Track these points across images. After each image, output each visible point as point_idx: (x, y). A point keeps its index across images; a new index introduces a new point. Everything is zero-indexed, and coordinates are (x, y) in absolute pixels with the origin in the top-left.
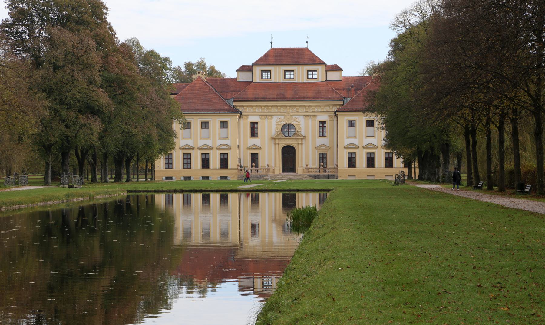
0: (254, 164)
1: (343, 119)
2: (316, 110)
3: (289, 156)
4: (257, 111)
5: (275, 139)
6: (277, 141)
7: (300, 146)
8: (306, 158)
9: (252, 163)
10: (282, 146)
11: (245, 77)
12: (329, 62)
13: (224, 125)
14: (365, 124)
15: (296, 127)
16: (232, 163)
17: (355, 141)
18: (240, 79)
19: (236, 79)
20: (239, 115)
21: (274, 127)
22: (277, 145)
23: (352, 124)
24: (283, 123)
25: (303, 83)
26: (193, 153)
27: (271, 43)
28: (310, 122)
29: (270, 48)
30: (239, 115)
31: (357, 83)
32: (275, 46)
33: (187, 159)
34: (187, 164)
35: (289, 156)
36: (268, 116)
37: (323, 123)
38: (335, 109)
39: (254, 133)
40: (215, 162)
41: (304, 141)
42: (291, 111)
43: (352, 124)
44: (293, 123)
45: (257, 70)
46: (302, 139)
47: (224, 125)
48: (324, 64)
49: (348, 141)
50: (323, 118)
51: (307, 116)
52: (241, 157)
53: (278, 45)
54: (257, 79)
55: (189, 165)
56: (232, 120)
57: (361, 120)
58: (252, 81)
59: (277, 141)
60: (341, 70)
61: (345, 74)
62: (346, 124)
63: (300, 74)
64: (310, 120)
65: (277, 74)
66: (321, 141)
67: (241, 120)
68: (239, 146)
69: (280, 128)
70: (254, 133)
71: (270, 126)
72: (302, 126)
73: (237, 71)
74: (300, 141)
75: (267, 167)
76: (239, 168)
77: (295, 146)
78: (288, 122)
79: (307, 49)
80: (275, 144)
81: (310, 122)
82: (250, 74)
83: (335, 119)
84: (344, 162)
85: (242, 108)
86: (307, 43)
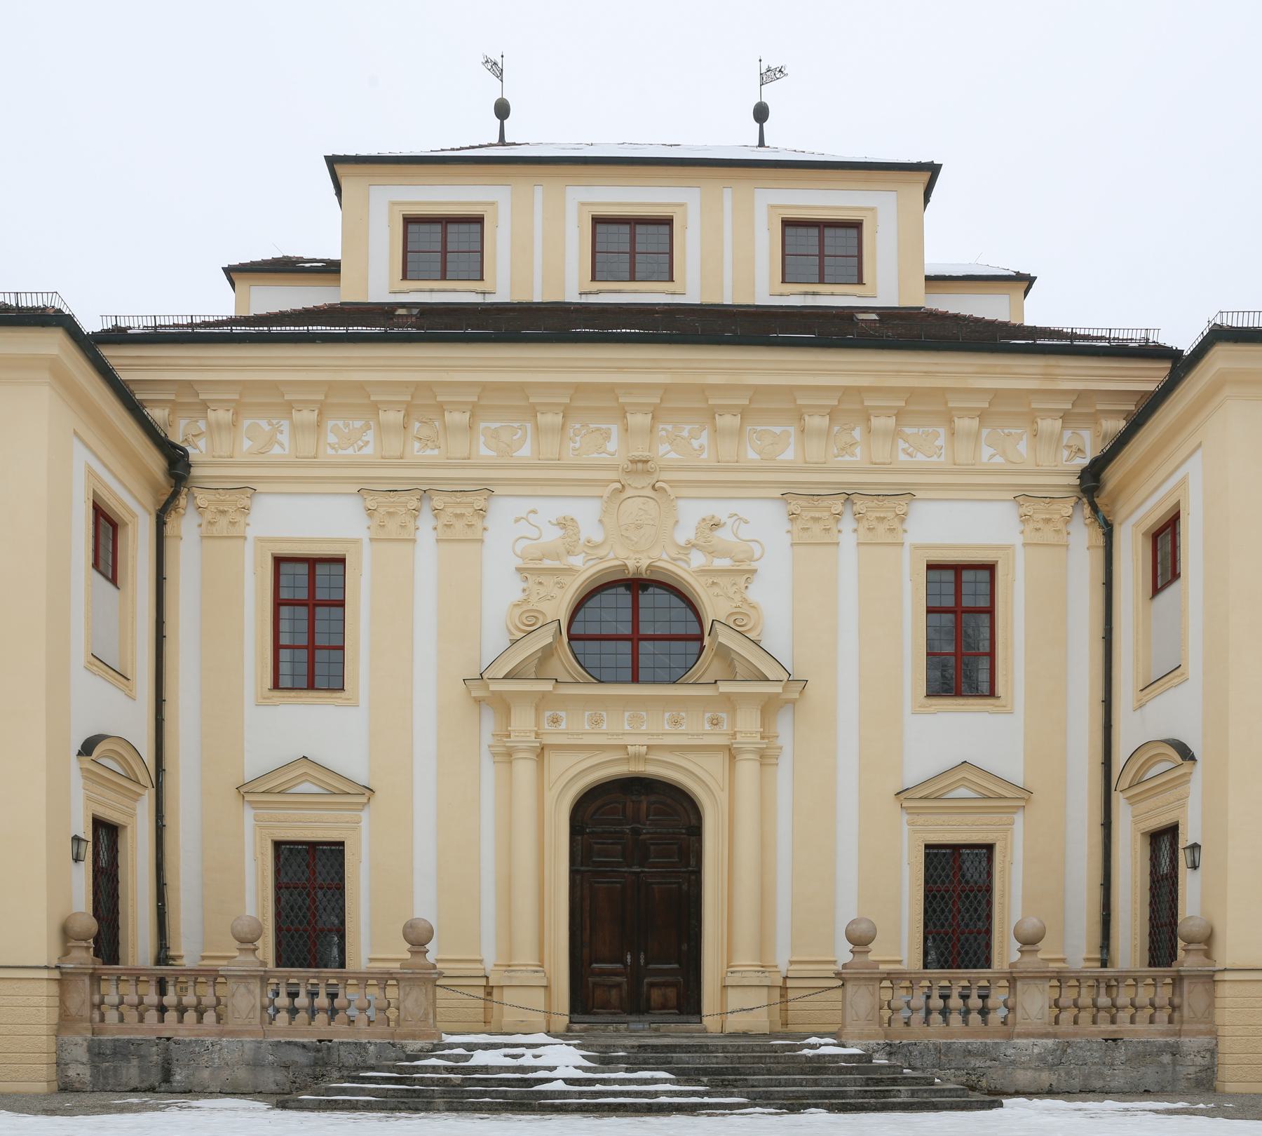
3: (636, 880)
5: (503, 705)
6: (523, 722)
7: (747, 769)
10: (573, 775)
15: (713, 606)
22: (524, 769)
24: (585, 569)
27: (502, 110)
35: (636, 880)
41: (784, 728)
44: (688, 569)
46: (769, 708)
51: (819, 503)
59: (523, 722)
71: (457, 594)
74: (748, 723)
78: (637, 561)
80: (507, 756)
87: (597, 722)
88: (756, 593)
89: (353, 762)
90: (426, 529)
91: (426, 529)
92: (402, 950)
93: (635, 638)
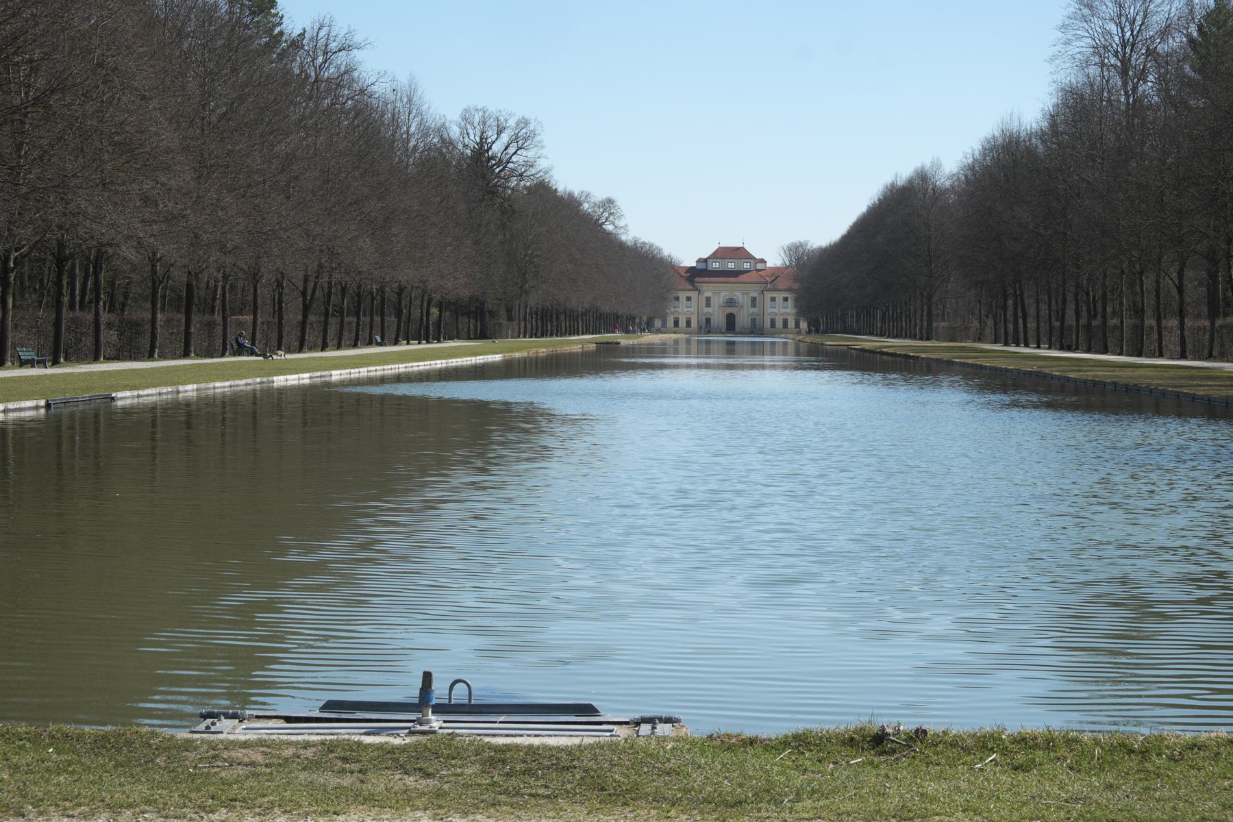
1: (768, 295)
8: (743, 319)
11: (702, 266)
12: (758, 257)
16: (694, 324)
17: (776, 310)
23: (773, 299)
31: (776, 273)
37: (754, 299)
39: (708, 305)
40: (682, 323)
47: (689, 299)
49: (770, 310)
50: (755, 294)
53: (723, 245)
56: (693, 295)
57: (780, 296)
66: (755, 310)
70: (708, 305)
84: (767, 324)
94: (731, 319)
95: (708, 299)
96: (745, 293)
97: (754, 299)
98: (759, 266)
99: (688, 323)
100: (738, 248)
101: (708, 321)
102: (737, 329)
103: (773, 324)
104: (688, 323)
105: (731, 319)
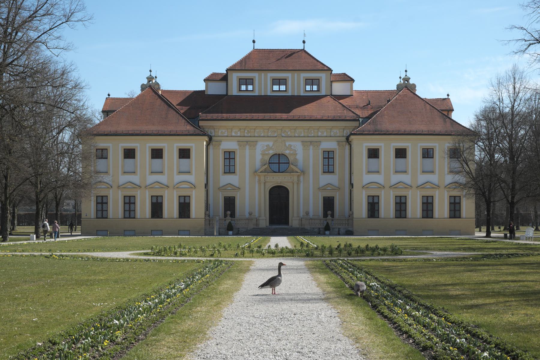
0: (229, 213)
2: (320, 134)
4: (233, 134)
9: (226, 210)
10: (269, 186)
11: (217, 89)
13: (184, 154)
14: (393, 154)
15: (291, 158)
16: (197, 209)
18: (210, 92)
19: (204, 91)
20: (206, 138)
21: (259, 157)
23: (374, 154)
24: (271, 152)
25: (299, 97)
26: (138, 194)
27: (254, 42)
28: (311, 151)
29: (252, 49)
30: (206, 138)
32: (258, 46)
33: (130, 203)
34: (130, 211)
36: (248, 142)
38: (347, 132)
42: (283, 135)
43: (374, 154)
44: (287, 152)
45: (234, 78)
47: (184, 154)
48: (330, 70)
50: (330, 145)
52: (211, 202)
54: (234, 91)
55: (132, 213)
58: (227, 95)
60: (352, 80)
61: (357, 86)
62: (365, 153)
63: (296, 85)
64: (311, 147)
65: (263, 85)
67: (211, 147)
68: (206, 185)
69: (267, 158)
72: (300, 157)
73: (205, 80)
75: (247, 215)
76: (207, 218)
77: (288, 186)
79: (303, 50)
81: (311, 151)
82: (223, 84)
83: (347, 147)
84: (361, 209)
85: (213, 131)
86: (304, 42)
87: (273, 178)
88: (298, 157)
89: (236, 184)
90: (247, 147)
91: (247, 147)
92: (247, 215)
93: (279, 163)
94: (279, 199)
95: (229, 156)
96: (310, 142)
97: (328, 156)
98: (339, 88)
99: (184, 209)
100: (290, 54)
101: (230, 203)
102: (294, 222)
103: (373, 208)
104: (184, 209)
105: (279, 199)
